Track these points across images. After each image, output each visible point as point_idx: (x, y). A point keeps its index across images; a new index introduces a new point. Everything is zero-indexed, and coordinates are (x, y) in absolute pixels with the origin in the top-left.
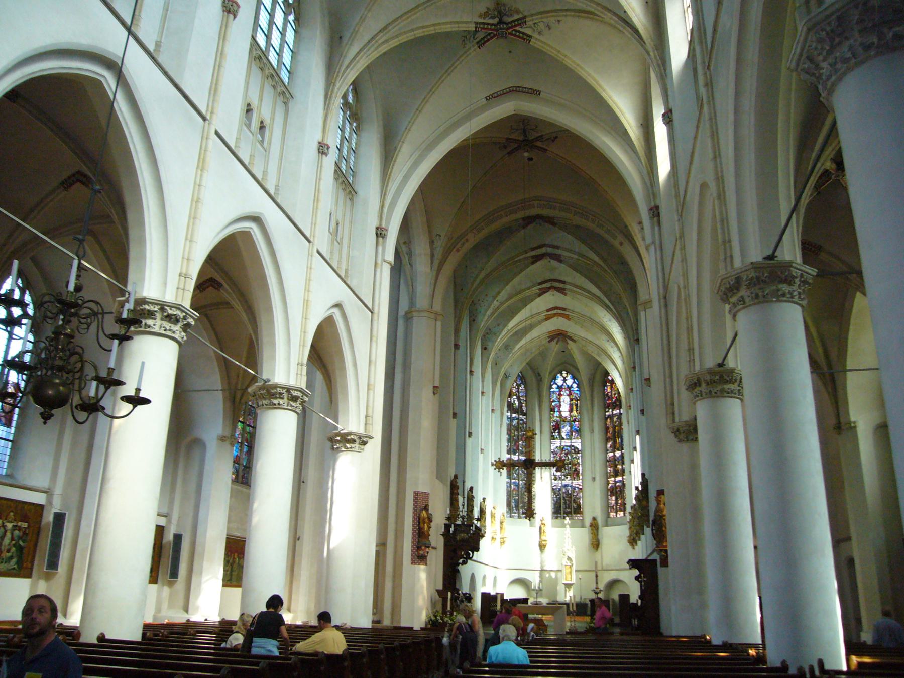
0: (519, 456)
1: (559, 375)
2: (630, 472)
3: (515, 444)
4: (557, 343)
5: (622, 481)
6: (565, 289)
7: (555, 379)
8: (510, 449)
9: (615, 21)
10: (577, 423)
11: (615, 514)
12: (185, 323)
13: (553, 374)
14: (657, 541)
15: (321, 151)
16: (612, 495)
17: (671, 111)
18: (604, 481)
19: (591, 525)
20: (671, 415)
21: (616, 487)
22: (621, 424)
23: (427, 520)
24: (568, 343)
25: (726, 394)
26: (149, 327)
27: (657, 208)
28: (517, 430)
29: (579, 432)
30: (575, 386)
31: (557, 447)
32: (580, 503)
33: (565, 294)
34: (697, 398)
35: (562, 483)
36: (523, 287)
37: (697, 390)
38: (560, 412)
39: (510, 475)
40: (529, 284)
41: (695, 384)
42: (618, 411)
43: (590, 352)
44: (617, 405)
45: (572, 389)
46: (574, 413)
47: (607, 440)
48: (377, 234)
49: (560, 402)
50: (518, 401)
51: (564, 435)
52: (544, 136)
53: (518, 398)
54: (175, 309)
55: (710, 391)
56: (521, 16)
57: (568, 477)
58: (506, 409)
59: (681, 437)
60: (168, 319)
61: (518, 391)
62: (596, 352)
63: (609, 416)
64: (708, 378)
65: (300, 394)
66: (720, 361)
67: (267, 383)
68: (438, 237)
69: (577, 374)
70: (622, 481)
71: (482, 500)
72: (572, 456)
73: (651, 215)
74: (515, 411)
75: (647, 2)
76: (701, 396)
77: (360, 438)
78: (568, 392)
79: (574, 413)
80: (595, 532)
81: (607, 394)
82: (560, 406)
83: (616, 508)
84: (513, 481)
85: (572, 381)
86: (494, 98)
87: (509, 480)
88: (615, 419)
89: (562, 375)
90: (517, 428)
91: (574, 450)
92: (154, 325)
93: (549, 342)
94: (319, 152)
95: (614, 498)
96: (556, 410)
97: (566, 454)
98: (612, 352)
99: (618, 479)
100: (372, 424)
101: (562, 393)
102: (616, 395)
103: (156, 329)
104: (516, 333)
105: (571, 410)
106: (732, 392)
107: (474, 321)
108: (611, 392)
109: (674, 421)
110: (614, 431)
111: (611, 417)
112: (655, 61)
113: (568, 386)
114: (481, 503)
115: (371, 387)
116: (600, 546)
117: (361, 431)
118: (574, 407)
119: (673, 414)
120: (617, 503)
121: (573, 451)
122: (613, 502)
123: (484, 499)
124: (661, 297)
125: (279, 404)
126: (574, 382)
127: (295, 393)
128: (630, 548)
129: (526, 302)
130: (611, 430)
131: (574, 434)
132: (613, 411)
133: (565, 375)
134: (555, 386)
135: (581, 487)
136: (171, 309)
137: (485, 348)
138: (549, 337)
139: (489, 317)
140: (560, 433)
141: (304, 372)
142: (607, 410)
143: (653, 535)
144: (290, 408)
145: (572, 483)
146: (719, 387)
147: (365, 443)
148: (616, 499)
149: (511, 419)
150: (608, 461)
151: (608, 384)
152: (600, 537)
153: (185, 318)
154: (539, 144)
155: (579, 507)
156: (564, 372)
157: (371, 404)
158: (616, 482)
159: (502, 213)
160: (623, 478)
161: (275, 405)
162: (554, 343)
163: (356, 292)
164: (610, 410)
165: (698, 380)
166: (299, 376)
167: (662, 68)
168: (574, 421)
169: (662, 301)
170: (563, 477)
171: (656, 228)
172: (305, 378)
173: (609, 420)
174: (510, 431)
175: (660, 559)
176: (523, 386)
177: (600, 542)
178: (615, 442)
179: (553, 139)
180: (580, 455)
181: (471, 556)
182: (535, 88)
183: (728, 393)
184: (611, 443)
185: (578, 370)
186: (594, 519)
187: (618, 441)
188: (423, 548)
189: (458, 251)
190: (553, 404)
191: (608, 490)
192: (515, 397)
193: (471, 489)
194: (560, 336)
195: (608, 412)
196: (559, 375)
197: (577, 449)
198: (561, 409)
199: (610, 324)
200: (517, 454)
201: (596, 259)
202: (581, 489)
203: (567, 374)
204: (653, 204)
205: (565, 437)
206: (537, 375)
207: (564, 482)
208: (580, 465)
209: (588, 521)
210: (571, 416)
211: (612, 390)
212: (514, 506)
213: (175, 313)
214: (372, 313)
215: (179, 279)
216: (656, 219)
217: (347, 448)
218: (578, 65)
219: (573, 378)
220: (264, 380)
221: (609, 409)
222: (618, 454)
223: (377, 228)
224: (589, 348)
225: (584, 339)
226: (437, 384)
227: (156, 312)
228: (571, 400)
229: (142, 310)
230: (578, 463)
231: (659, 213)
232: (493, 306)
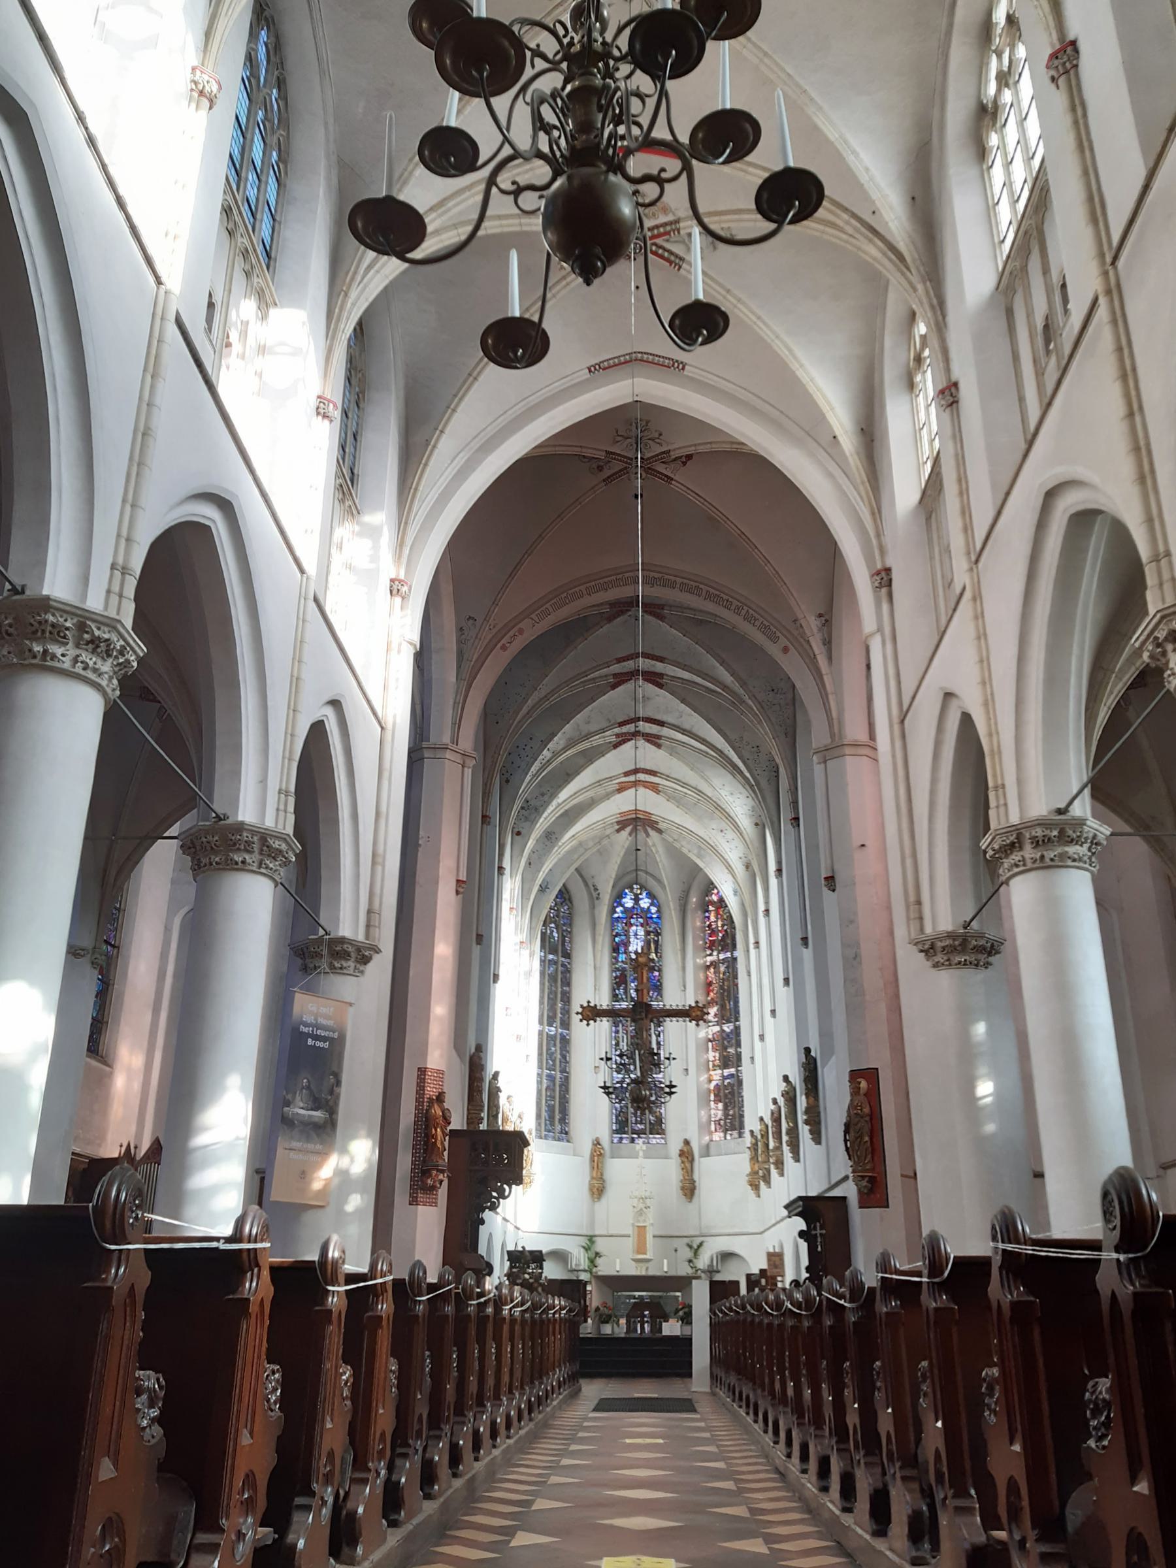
2: (752, 1058)
4: (630, 834)
6: (659, 737)
9: (855, 229)
11: (722, 1135)
12: (121, 660)
14: (855, 1162)
15: (322, 411)
17: (956, 385)
19: (682, 1154)
20: (917, 922)
23: (441, 1121)
24: (648, 835)
25: (1070, 863)
26: (54, 657)
27: (888, 570)
30: (654, 909)
32: (661, 1114)
33: (659, 746)
34: (1016, 870)
36: (593, 727)
37: (1015, 857)
40: (605, 724)
41: (1012, 844)
42: (729, 955)
43: (685, 851)
48: (391, 592)
49: (627, 935)
52: (672, 453)
54: (106, 629)
55: (1042, 857)
56: (670, 218)
59: (939, 958)
60: (91, 646)
62: (695, 852)
63: (712, 963)
64: (1039, 832)
65: (284, 847)
66: (1062, 805)
67: (222, 822)
68: (471, 621)
73: (877, 584)
75: (913, 198)
76: (1024, 865)
77: (359, 950)
80: (688, 1165)
81: (710, 926)
86: (604, 369)
89: (631, 891)
92: (63, 655)
93: (618, 831)
94: (318, 414)
95: (720, 1105)
96: (622, 949)
98: (728, 850)
100: (379, 928)
102: (725, 927)
103: (67, 664)
104: (566, 813)
106: (1080, 860)
107: (507, 781)
108: (716, 922)
109: (922, 930)
112: (925, 300)
115: (380, 860)
116: (697, 1192)
117: (361, 937)
118: (652, 946)
119: (921, 918)
120: (726, 1115)
122: (720, 1114)
124: (896, 720)
125: (243, 862)
126: (652, 904)
127: (276, 844)
129: (589, 757)
132: (719, 953)
134: (619, 909)
136: (99, 629)
137: (519, 833)
138: (618, 823)
139: (534, 776)
141: (291, 808)
143: (847, 1149)
144: (263, 871)
146: (1059, 850)
147: (365, 960)
148: (726, 1108)
152: (696, 1177)
153: (122, 652)
154: (661, 468)
155: (659, 1121)
157: (377, 890)
158: (724, 1078)
159: (582, 588)
160: (737, 1071)
161: (237, 863)
162: (625, 833)
163: (364, 684)
164: (715, 953)
165: (1019, 837)
166: (282, 814)
167: (939, 313)
169: (896, 727)
171: (885, 607)
172: (291, 818)
173: (712, 970)
175: (860, 1192)
177: (697, 1184)
179: (684, 459)
181: (507, 1194)
182: (676, 358)
183: (1074, 860)
185: (659, 881)
186: (687, 1142)
187: (730, 1005)
188: (434, 1172)
189: (504, 648)
193: (496, 1076)
194: (637, 822)
195: (711, 955)
199: (731, 800)
201: (728, 678)
204: (879, 566)
206: (592, 888)
209: (675, 1146)
211: (717, 918)
213: (106, 636)
214: (382, 728)
215: (111, 576)
216: (884, 590)
217: (335, 968)
218: (759, 318)
219: (651, 895)
220: (218, 816)
221: (712, 951)
223: (392, 581)
224: (684, 843)
225: (679, 826)
226: (463, 877)
227: (67, 629)
228: (648, 933)
229: (40, 623)
231: (890, 580)
232: (541, 757)
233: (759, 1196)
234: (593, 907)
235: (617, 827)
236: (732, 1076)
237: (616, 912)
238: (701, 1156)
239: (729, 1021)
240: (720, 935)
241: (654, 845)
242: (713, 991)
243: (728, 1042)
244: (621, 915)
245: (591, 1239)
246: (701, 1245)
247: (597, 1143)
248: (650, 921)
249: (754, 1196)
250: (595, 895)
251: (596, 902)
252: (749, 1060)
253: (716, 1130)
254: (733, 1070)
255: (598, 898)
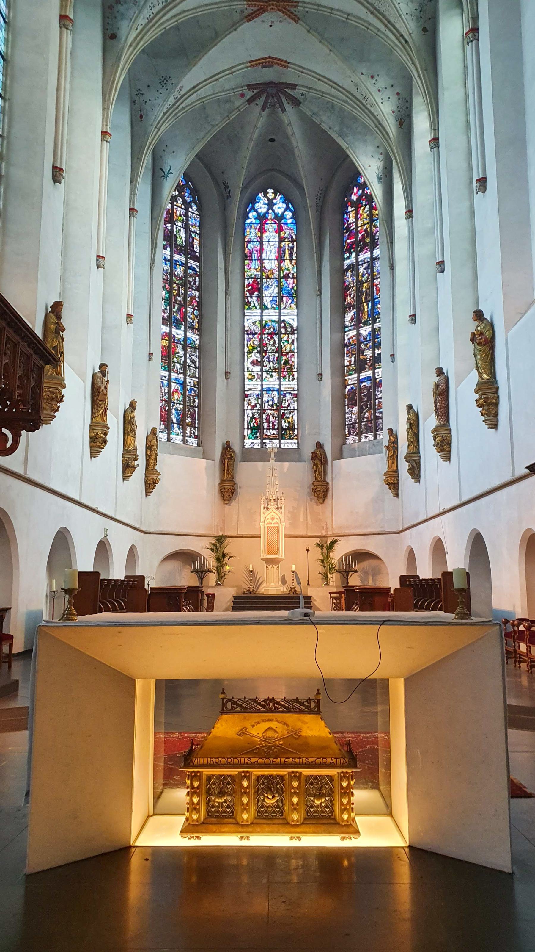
0: (185, 331)
1: (261, 195)
2: (393, 356)
3: (179, 310)
4: (263, 109)
5: (373, 379)
7: (253, 201)
8: (170, 316)
10: (290, 281)
11: (356, 438)
13: (247, 195)
16: (351, 406)
18: (338, 380)
19: (314, 457)
21: (360, 390)
22: (373, 277)
24: (283, 110)
28: (184, 285)
29: (295, 295)
30: (289, 215)
31: (254, 323)
35: (262, 385)
38: (261, 260)
39: (169, 366)
42: (368, 255)
43: (325, 127)
44: (366, 244)
45: (283, 221)
46: (287, 264)
47: (345, 310)
49: (261, 242)
50: (186, 232)
51: (267, 301)
53: (186, 227)
57: (274, 374)
58: (161, 242)
61: (186, 215)
63: (349, 267)
69: (295, 193)
70: (373, 379)
71: (97, 370)
72: (280, 339)
74: (181, 250)
78: (275, 226)
79: (287, 264)
81: (348, 228)
82: (262, 250)
83: (360, 427)
84: (174, 375)
85: (284, 206)
87: (166, 374)
88: (361, 269)
89: (265, 195)
90: (184, 283)
91: (286, 328)
95: (355, 409)
96: (255, 256)
97: (271, 335)
98: (379, 101)
99: (363, 375)
101: (266, 227)
105: (280, 259)
108: (356, 222)
110: (359, 291)
111: (354, 267)
113: (276, 215)
114: (94, 376)
118: (287, 253)
120: (361, 418)
121: (283, 331)
122: (354, 417)
123: (103, 366)
126: (287, 209)
128: (390, 494)
130: (353, 292)
131: (284, 299)
132: (357, 256)
133: (271, 195)
134: (252, 214)
135: (296, 392)
140: (260, 298)
142: (346, 255)
145: (280, 385)
148: (361, 410)
149: (173, 263)
150: (345, 346)
151: (350, 209)
152: (329, 479)
156: (270, 191)
158: (360, 381)
160: (374, 373)
164: (354, 255)
168: (287, 277)
170: (265, 374)
173: (349, 273)
174: (171, 286)
176: (195, 208)
177: (330, 486)
178: (360, 310)
180: (295, 337)
184: (352, 314)
186: (319, 446)
190: (250, 246)
191: (344, 396)
192: (180, 224)
195: (348, 258)
196: (261, 195)
197: (292, 327)
198: (264, 255)
200: (183, 328)
202: (296, 396)
203: (275, 193)
205: (269, 306)
207: (267, 384)
208: (296, 355)
209: (309, 449)
210: (280, 268)
211: (357, 219)
212: (175, 421)
219: (287, 200)
222: (365, 331)
224: (324, 118)
228: (281, 240)
230: (292, 351)
233: (397, 495)
234: (224, 208)
235: (249, 94)
236: (368, 379)
237: (249, 218)
238: (335, 458)
239: (366, 323)
240: (360, 235)
241: (290, 124)
242: (350, 294)
243: (366, 345)
244: (254, 221)
245: (220, 539)
246: (333, 543)
247: (227, 447)
248: (284, 227)
249: (392, 495)
250: (225, 193)
251: (228, 201)
252: (389, 359)
253: (350, 434)
254: (369, 373)
255: (228, 197)
